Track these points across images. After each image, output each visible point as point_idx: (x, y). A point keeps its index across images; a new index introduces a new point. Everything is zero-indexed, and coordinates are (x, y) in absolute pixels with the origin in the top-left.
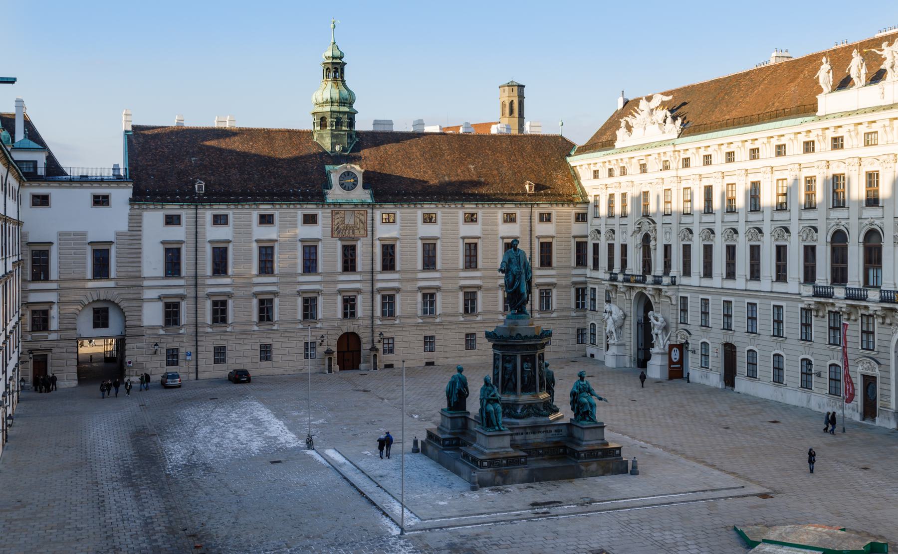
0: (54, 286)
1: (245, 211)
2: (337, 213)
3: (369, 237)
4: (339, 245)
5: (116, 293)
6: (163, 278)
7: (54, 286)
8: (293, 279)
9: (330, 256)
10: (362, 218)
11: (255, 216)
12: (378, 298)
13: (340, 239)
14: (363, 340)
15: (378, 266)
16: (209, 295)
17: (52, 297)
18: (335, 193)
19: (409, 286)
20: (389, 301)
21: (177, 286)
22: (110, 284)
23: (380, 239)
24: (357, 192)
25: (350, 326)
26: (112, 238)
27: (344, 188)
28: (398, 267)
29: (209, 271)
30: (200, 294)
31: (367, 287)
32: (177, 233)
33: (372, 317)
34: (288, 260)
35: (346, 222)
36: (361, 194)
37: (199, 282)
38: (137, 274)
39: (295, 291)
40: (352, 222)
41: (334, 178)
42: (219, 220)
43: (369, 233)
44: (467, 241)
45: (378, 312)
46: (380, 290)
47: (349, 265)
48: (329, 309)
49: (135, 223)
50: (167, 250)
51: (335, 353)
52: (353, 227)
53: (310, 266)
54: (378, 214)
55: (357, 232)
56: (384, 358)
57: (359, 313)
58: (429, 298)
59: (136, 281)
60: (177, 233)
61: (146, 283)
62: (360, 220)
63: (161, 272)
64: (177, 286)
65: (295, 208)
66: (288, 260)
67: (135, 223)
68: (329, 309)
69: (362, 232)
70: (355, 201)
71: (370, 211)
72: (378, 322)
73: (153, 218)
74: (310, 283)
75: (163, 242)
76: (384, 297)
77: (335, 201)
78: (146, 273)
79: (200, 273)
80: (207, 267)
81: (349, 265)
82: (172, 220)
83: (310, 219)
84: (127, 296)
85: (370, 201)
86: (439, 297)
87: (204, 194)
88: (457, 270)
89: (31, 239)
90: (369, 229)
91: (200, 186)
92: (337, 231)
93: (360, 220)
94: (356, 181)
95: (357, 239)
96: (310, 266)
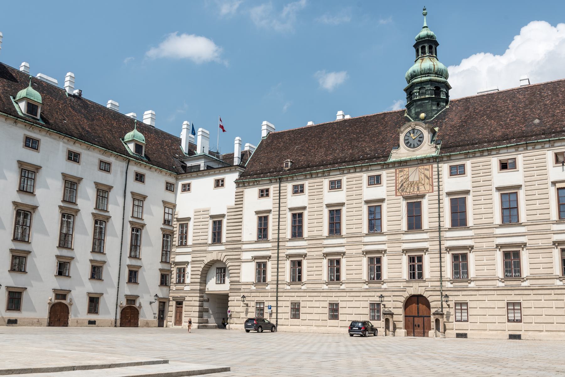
0: (189, 250)
1: (318, 180)
2: (401, 171)
3: (437, 193)
4: (404, 204)
5: (224, 254)
6: (256, 242)
7: (189, 250)
8: (358, 239)
9: (394, 215)
10: (427, 173)
11: (326, 182)
12: (448, 258)
13: (405, 198)
14: (432, 304)
15: (447, 222)
16: (289, 256)
17: (188, 258)
18: (402, 153)
19: (485, 244)
20: (460, 260)
21: (266, 248)
22: (222, 248)
23: (448, 194)
24: (423, 149)
25: (416, 288)
26: (224, 211)
27: (410, 147)
28: (470, 222)
29: (289, 235)
30: (280, 255)
31: (433, 246)
32: (267, 204)
33: (441, 280)
34: (355, 220)
35: (411, 179)
36: (427, 149)
37: (281, 244)
38: (238, 239)
39: (360, 251)
40: (417, 179)
41: (402, 137)
42: (298, 190)
43: (436, 188)
44: (559, 185)
45: (448, 272)
46: (449, 249)
47: (415, 223)
48: (395, 269)
49: (239, 198)
50: (260, 218)
51: (401, 318)
52: (418, 184)
53: (374, 225)
54: (445, 168)
55: (422, 188)
56: (454, 327)
57: (427, 274)
58: (512, 259)
59: (237, 244)
60: (267, 204)
61: (244, 247)
62: (425, 176)
63: (255, 238)
64: (266, 248)
65: (361, 171)
66: (355, 220)
67: (239, 198)
68: (395, 269)
69: (428, 187)
70: (419, 156)
71: (435, 165)
72: (448, 285)
73: (251, 193)
74: (375, 242)
75: (257, 213)
76: (455, 257)
77: (398, 159)
78: (245, 238)
79: (281, 236)
80: (287, 232)
81: (415, 223)
82: (264, 193)
83: (376, 181)
84: (231, 257)
85: (434, 154)
86: (525, 256)
87: (288, 170)
88: (548, 221)
89: (179, 217)
90: (436, 184)
91: (288, 164)
92: (400, 189)
93: (425, 176)
94: (422, 137)
95: (423, 196)
96: (374, 225)
